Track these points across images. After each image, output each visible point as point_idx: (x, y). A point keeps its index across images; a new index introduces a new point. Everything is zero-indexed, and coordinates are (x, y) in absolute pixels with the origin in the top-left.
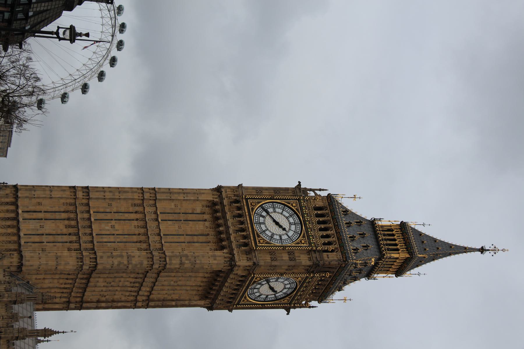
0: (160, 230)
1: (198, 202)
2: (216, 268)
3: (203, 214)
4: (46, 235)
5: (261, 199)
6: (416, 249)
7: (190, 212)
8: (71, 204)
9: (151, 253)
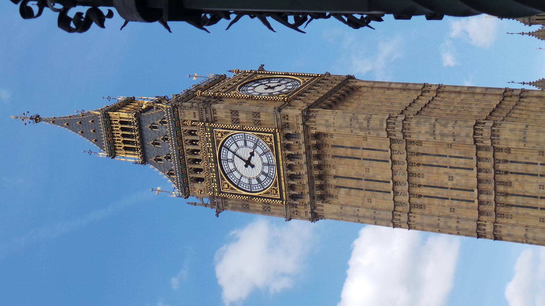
0: (392, 169)
1: (343, 203)
2: (329, 111)
3: (337, 187)
4: (537, 175)
5: (264, 198)
6: (101, 122)
7: (353, 191)
8: (502, 216)
9: (404, 136)
